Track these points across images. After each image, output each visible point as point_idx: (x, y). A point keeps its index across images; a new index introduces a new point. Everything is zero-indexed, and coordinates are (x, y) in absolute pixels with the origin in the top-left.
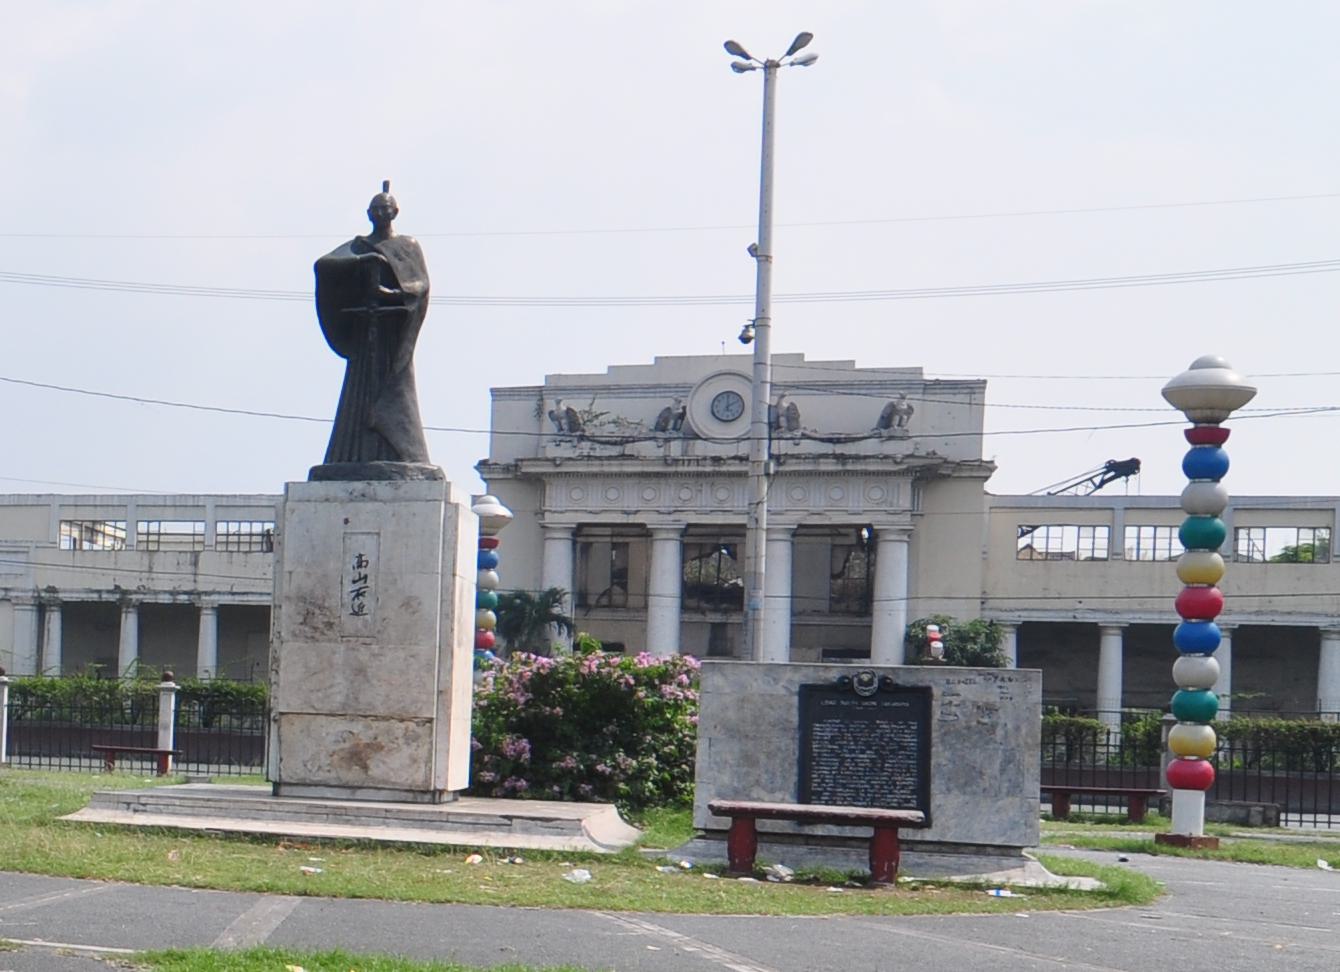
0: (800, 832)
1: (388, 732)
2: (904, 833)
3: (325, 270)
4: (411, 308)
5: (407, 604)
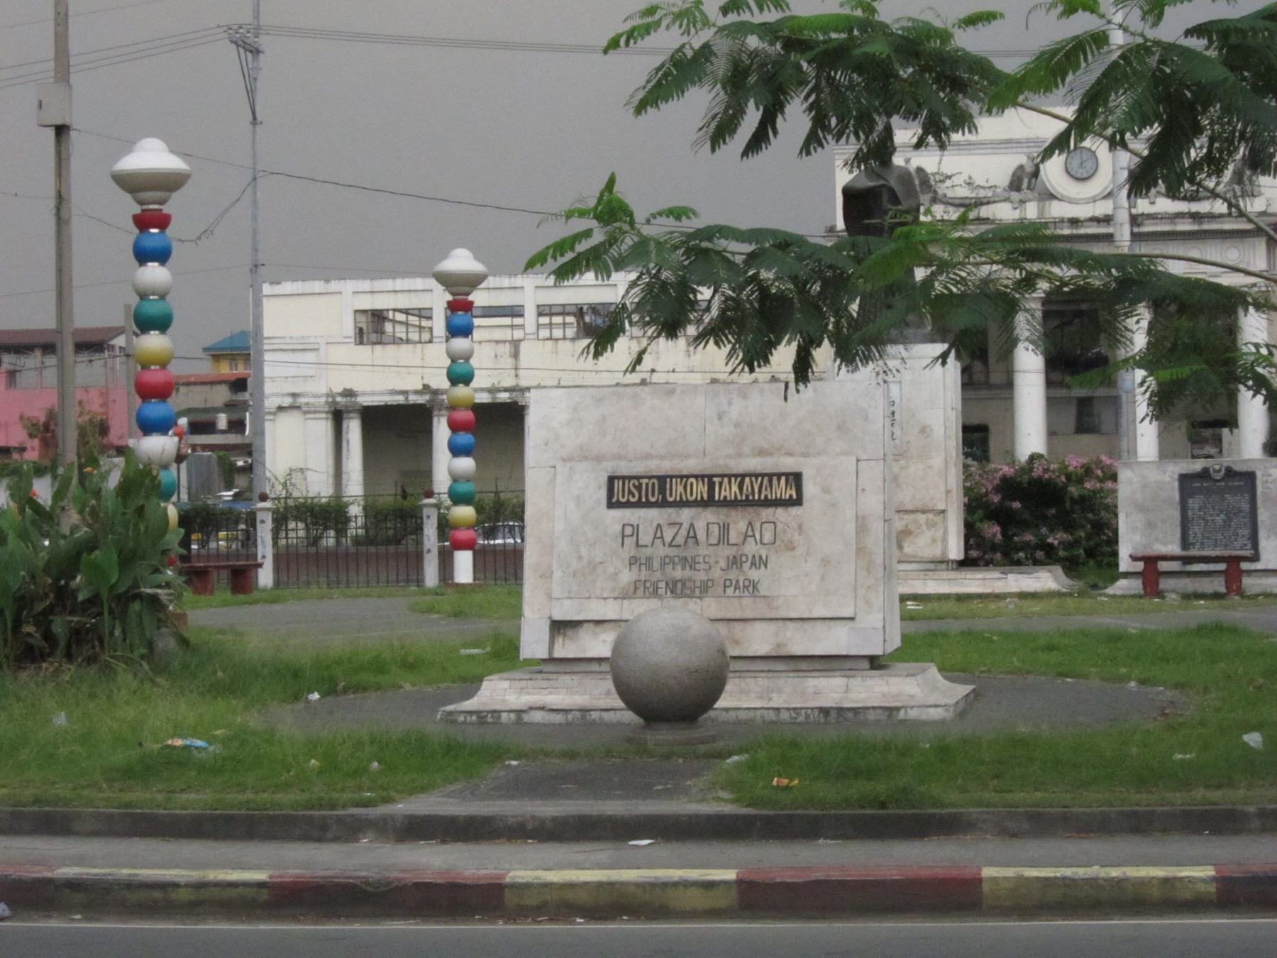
2: (1245, 566)
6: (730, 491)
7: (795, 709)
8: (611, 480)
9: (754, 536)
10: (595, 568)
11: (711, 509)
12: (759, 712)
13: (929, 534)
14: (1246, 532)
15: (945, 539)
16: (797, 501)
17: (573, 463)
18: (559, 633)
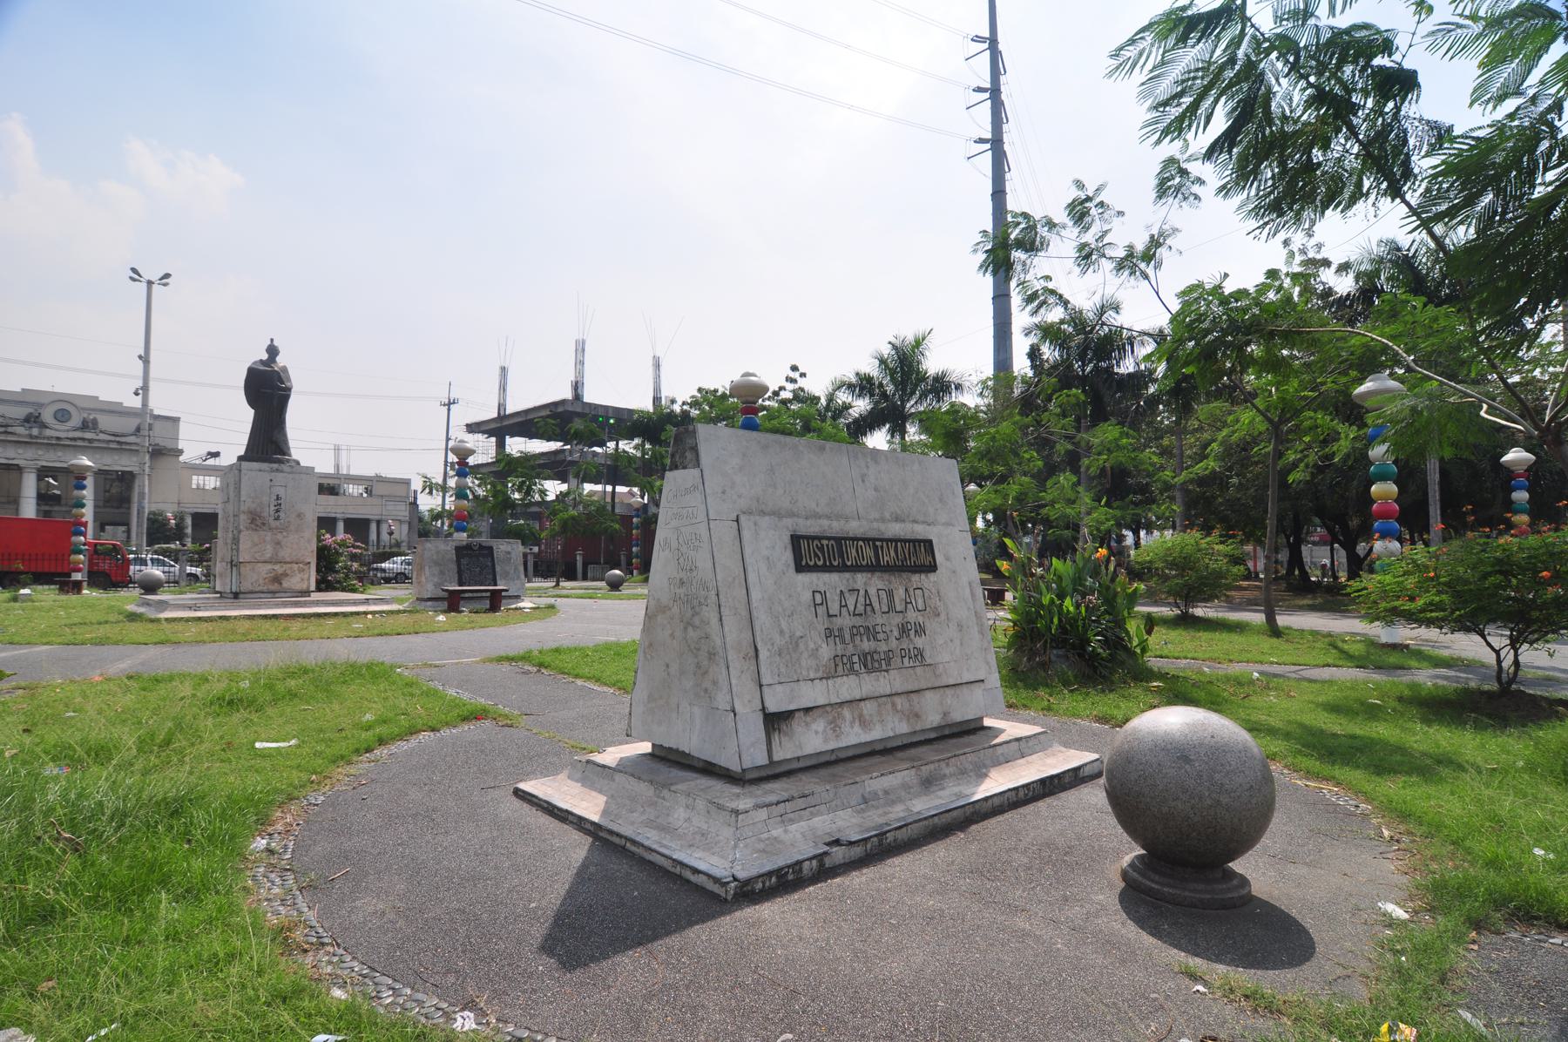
2: (503, 594)
6: (888, 557)
10: (797, 645)
11: (878, 574)
13: (299, 576)
14: (491, 576)
15: (309, 579)
16: (932, 568)
18: (774, 730)
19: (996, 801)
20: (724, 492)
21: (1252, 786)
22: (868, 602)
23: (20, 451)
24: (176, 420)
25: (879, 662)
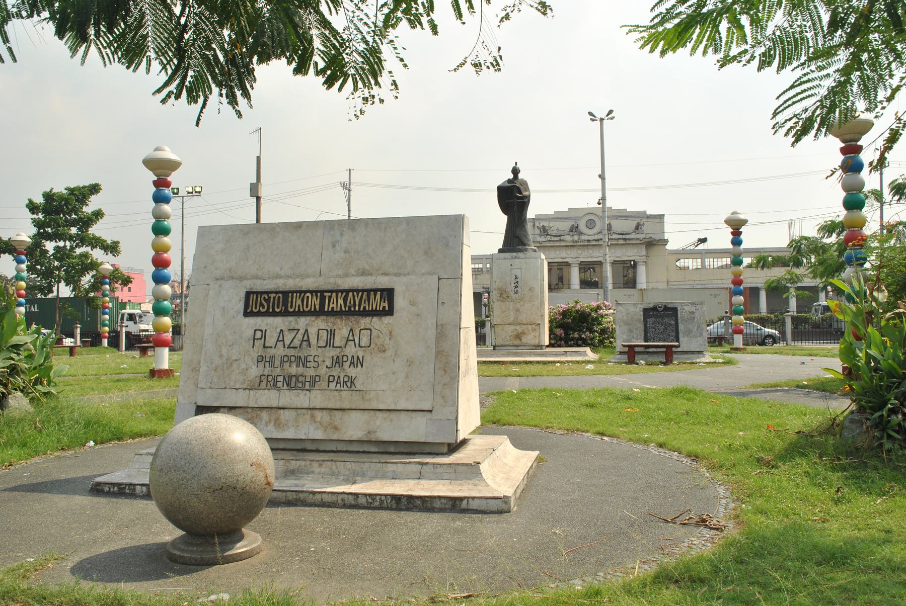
0: (646, 351)
1: (527, 328)
2: (674, 349)
3: (500, 189)
4: (526, 200)
5: (530, 289)
6: (338, 303)
7: (370, 495)
8: (248, 294)
9: (354, 340)
10: (231, 365)
11: (322, 317)
12: (340, 497)
13: (533, 334)
14: (674, 334)
16: (390, 312)
17: (223, 282)
19: (327, 498)
20: (205, 267)
21: (162, 469)
22: (306, 338)
23: (569, 252)
24: (661, 217)
25: (304, 384)
